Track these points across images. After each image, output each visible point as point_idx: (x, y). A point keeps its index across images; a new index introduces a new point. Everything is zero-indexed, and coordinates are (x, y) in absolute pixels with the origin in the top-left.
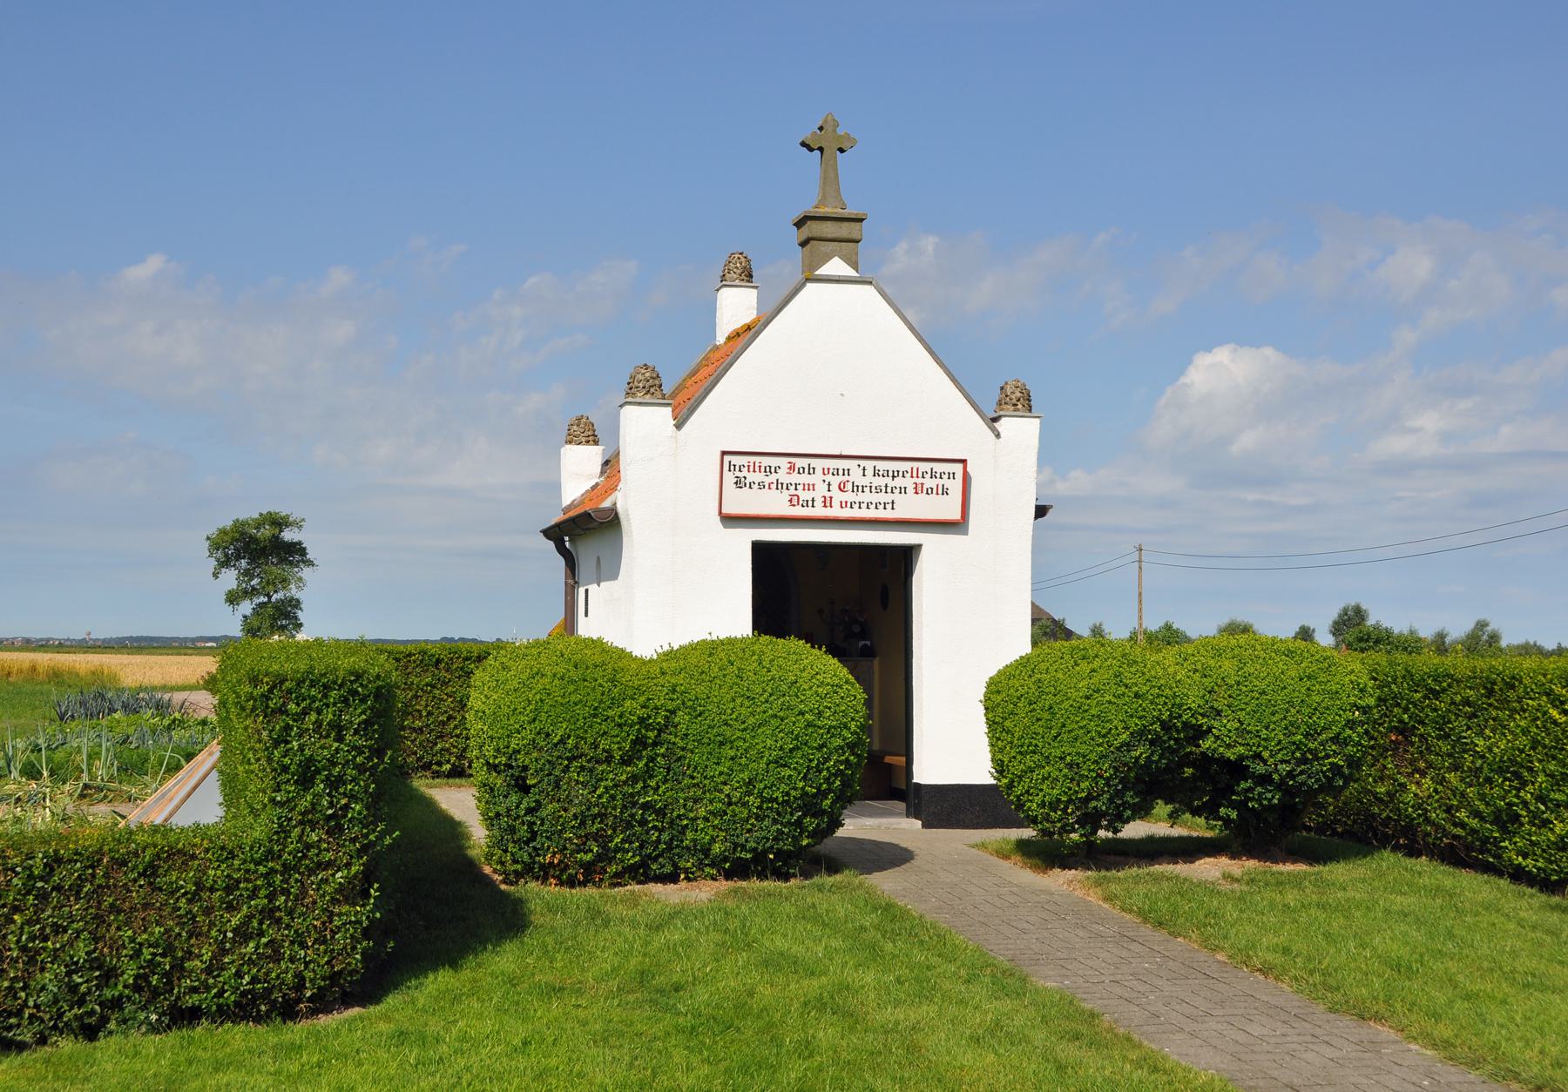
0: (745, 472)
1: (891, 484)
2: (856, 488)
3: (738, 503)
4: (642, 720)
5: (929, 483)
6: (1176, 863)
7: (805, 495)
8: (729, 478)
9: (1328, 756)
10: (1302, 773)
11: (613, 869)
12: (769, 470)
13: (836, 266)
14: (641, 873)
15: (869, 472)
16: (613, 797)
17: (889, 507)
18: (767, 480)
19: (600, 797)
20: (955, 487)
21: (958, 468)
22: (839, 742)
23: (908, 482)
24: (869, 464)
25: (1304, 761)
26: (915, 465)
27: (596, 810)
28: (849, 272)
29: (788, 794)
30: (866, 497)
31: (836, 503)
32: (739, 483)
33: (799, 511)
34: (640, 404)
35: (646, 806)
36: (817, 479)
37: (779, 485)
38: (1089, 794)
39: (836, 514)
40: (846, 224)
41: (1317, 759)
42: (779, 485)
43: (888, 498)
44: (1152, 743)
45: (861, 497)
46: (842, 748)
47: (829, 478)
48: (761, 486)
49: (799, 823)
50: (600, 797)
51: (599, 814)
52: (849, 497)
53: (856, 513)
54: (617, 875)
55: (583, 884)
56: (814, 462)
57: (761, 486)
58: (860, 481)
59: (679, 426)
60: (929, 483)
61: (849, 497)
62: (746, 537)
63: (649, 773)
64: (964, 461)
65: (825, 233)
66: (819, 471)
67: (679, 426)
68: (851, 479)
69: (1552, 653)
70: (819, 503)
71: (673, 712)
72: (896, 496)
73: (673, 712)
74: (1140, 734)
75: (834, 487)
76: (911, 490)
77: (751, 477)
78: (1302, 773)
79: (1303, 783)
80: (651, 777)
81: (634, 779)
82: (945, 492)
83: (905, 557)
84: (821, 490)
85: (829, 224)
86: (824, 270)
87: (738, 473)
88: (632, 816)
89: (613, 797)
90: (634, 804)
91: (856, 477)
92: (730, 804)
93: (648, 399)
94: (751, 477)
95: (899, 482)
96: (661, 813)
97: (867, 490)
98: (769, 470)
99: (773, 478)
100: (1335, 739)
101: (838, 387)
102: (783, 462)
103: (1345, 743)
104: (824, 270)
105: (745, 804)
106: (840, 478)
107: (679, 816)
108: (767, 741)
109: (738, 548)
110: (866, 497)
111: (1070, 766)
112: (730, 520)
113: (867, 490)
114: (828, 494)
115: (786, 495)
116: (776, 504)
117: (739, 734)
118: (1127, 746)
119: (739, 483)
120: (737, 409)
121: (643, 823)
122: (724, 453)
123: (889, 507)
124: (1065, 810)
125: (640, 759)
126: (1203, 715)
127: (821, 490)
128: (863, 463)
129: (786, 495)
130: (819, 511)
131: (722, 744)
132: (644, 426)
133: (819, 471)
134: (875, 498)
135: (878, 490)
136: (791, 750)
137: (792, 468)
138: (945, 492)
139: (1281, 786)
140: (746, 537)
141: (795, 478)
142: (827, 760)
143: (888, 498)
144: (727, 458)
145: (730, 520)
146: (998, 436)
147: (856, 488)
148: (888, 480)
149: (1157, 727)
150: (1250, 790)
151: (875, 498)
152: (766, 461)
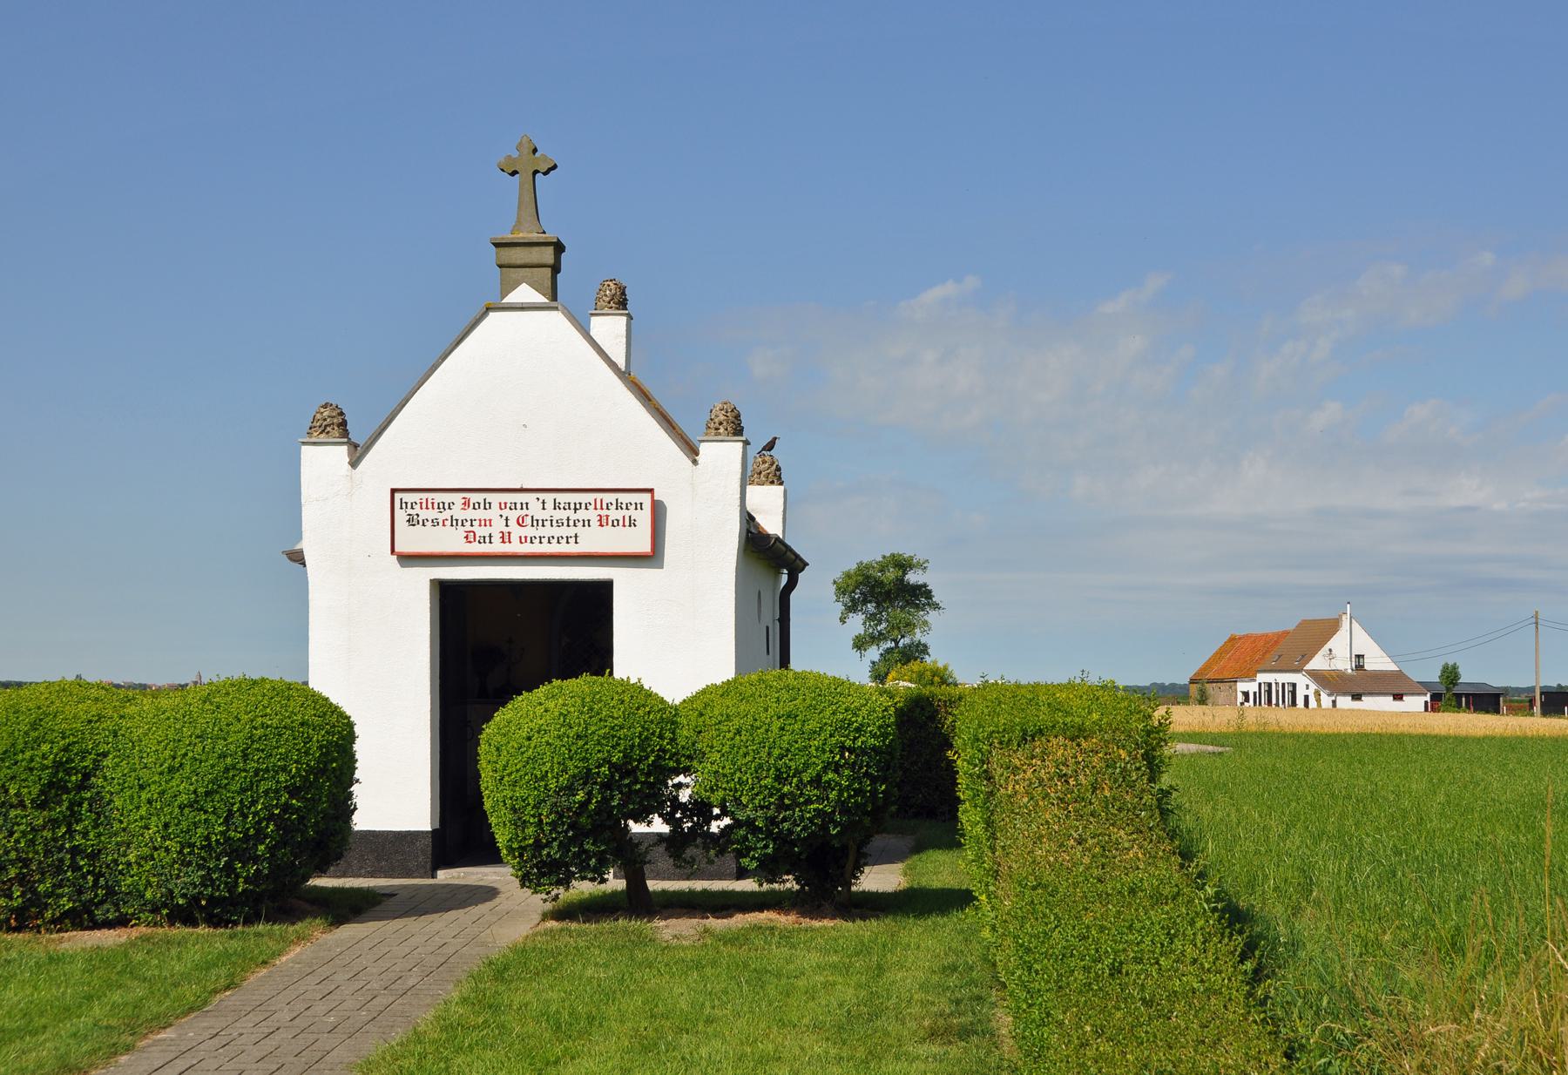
0: (417, 509)
1: (573, 517)
2: (535, 522)
3: (410, 541)
4: (58, 765)
5: (614, 514)
6: (731, 916)
7: (481, 531)
8: (401, 516)
9: (808, 802)
10: (784, 820)
11: (48, 915)
12: (442, 507)
13: (524, 293)
14: (82, 918)
15: (550, 505)
16: (32, 842)
17: (572, 540)
18: (441, 517)
19: (18, 841)
20: (644, 518)
21: (645, 499)
22: (271, 784)
23: (592, 515)
24: (549, 497)
25: (781, 807)
26: (599, 496)
27: (13, 855)
28: (540, 299)
29: (207, 838)
30: (547, 531)
31: (514, 538)
32: (411, 521)
33: (476, 548)
34: (314, 444)
35: (75, 851)
36: (493, 513)
37: (454, 522)
38: (537, 841)
39: (523, 549)
40: (536, 249)
41: (798, 805)
42: (454, 522)
43: (571, 531)
44: (606, 786)
45: (541, 531)
46: (277, 791)
47: (506, 513)
48: (435, 523)
49: (229, 868)
50: (18, 841)
51: (19, 859)
52: (529, 531)
53: (537, 548)
54: (54, 921)
55: (18, 929)
56: (490, 497)
57: (435, 523)
58: (540, 515)
59: (354, 464)
60: (614, 514)
61: (529, 531)
62: (423, 577)
63: (73, 816)
64: (651, 491)
65: (542, 263)
66: (495, 506)
67: (354, 464)
68: (530, 512)
69: (1065, 686)
70: (496, 538)
71: (105, 755)
72: (579, 529)
73: (105, 755)
74: (587, 777)
75: (512, 522)
76: (595, 523)
77: (424, 514)
78: (784, 820)
79: (790, 832)
80: (78, 821)
81: (54, 823)
82: (632, 523)
83: (603, 591)
84: (499, 525)
85: (518, 250)
86: (512, 298)
87: (410, 511)
88: (61, 861)
89: (32, 842)
90: (61, 849)
91: (535, 510)
92: (156, 849)
93: (323, 438)
94: (424, 514)
95: (582, 514)
96: (94, 856)
97: (547, 524)
98: (442, 507)
99: (447, 514)
100: (816, 781)
101: (527, 421)
102: (457, 498)
103: (829, 786)
104: (512, 298)
105: (167, 850)
106: (519, 513)
107: (115, 861)
108: (182, 788)
109: (416, 589)
110: (547, 531)
111: (514, 810)
112: (407, 559)
113: (547, 524)
114: (506, 530)
115: (461, 532)
116: (451, 541)
117: (156, 778)
118: (570, 789)
119: (411, 521)
120: (419, 443)
121: (75, 868)
122: (393, 491)
123: (572, 540)
124: (521, 856)
125: (59, 803)
126: (690, 758)
127: (499, 525)
128: (542, 496)
129: (461, 532)
130: (497, 547)
131: (142, 787)
132: (322, 463)
133: (495, 506)
134: (557, 532)
135: (560, 524)
136: (207, 794)
137: (466, 503)
138: (632, 523)
139: (769, 834)
140: (423, 577)
141: (470, 514)
142: (254, 803)
143: (571, 531)
144: (398, 496)
145: (407, 559)
146: (695, 462)
147: (535, 522)
148: (570, 513)
149: (605, 769)
150: (745, 838)
151: (557, 532)
152: (439, 497)
